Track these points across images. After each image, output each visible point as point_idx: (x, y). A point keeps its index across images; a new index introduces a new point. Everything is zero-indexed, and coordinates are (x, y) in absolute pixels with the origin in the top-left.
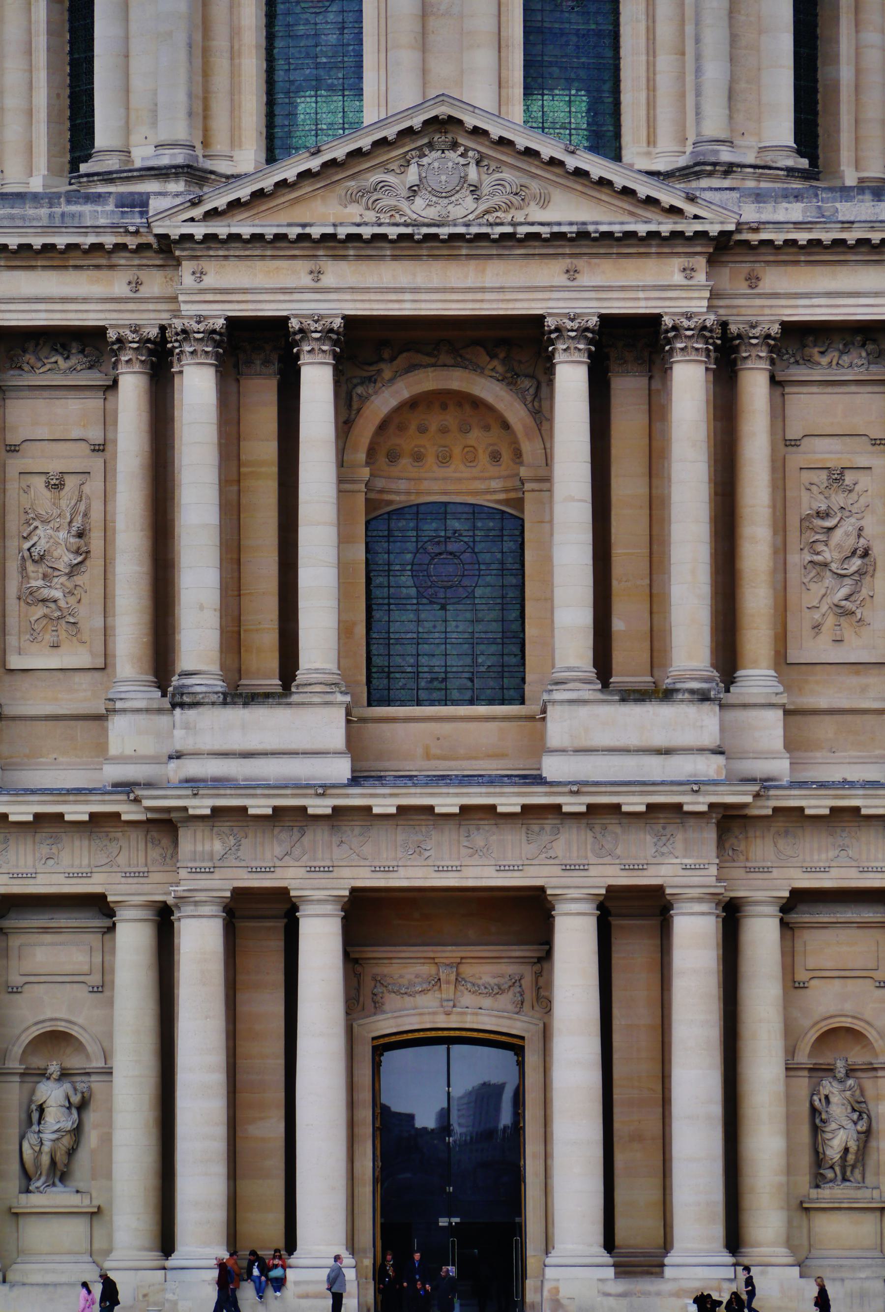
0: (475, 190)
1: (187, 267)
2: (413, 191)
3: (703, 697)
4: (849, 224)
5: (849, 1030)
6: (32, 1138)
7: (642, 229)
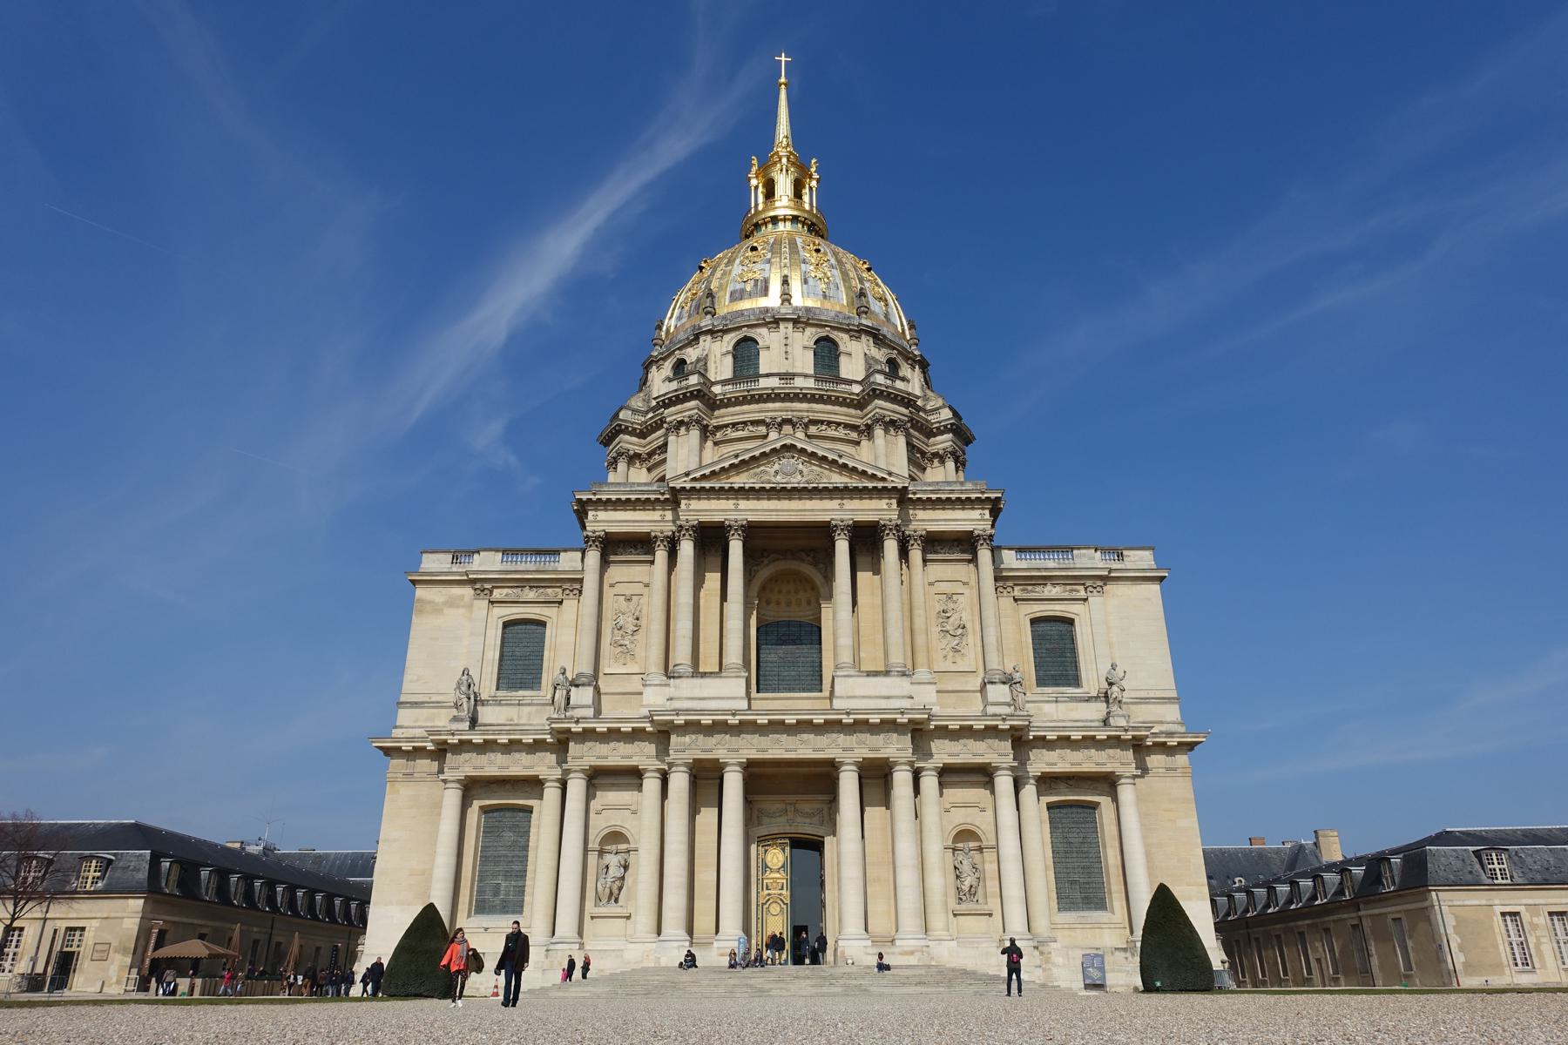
0: (801, 472)
1: (683, 502)
2: (776, 473)
3: (904, 674)
4: (952, 491)
5: (969, 831)
6: (602, 881)
7: (870, 485)
